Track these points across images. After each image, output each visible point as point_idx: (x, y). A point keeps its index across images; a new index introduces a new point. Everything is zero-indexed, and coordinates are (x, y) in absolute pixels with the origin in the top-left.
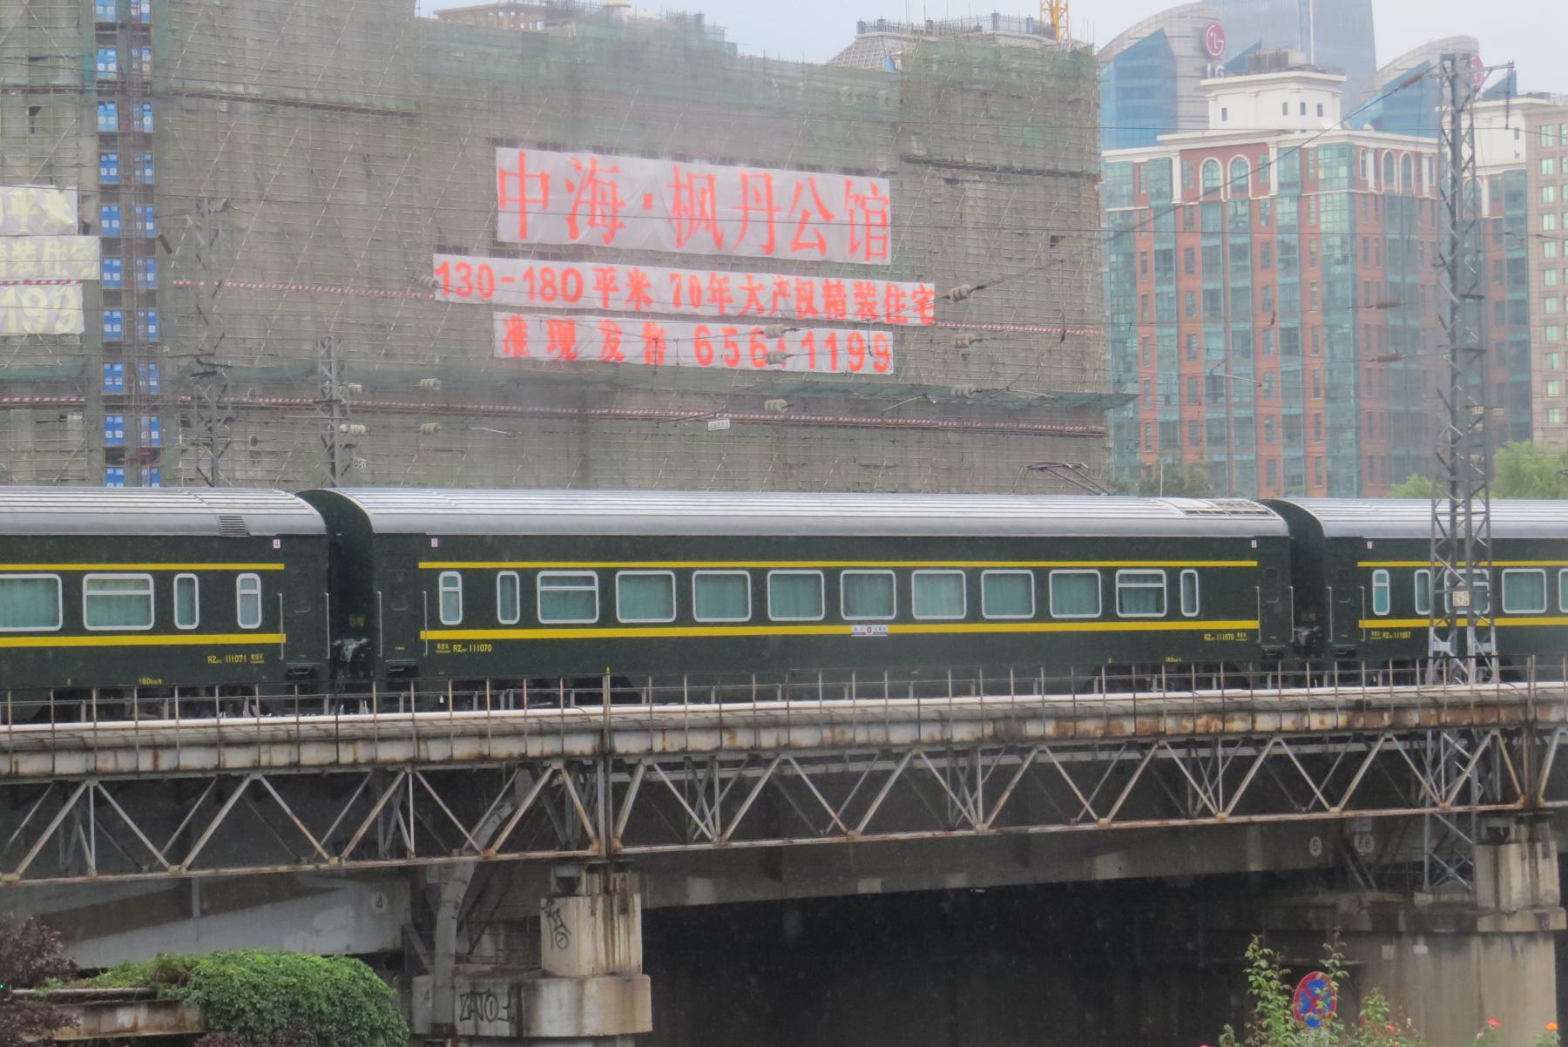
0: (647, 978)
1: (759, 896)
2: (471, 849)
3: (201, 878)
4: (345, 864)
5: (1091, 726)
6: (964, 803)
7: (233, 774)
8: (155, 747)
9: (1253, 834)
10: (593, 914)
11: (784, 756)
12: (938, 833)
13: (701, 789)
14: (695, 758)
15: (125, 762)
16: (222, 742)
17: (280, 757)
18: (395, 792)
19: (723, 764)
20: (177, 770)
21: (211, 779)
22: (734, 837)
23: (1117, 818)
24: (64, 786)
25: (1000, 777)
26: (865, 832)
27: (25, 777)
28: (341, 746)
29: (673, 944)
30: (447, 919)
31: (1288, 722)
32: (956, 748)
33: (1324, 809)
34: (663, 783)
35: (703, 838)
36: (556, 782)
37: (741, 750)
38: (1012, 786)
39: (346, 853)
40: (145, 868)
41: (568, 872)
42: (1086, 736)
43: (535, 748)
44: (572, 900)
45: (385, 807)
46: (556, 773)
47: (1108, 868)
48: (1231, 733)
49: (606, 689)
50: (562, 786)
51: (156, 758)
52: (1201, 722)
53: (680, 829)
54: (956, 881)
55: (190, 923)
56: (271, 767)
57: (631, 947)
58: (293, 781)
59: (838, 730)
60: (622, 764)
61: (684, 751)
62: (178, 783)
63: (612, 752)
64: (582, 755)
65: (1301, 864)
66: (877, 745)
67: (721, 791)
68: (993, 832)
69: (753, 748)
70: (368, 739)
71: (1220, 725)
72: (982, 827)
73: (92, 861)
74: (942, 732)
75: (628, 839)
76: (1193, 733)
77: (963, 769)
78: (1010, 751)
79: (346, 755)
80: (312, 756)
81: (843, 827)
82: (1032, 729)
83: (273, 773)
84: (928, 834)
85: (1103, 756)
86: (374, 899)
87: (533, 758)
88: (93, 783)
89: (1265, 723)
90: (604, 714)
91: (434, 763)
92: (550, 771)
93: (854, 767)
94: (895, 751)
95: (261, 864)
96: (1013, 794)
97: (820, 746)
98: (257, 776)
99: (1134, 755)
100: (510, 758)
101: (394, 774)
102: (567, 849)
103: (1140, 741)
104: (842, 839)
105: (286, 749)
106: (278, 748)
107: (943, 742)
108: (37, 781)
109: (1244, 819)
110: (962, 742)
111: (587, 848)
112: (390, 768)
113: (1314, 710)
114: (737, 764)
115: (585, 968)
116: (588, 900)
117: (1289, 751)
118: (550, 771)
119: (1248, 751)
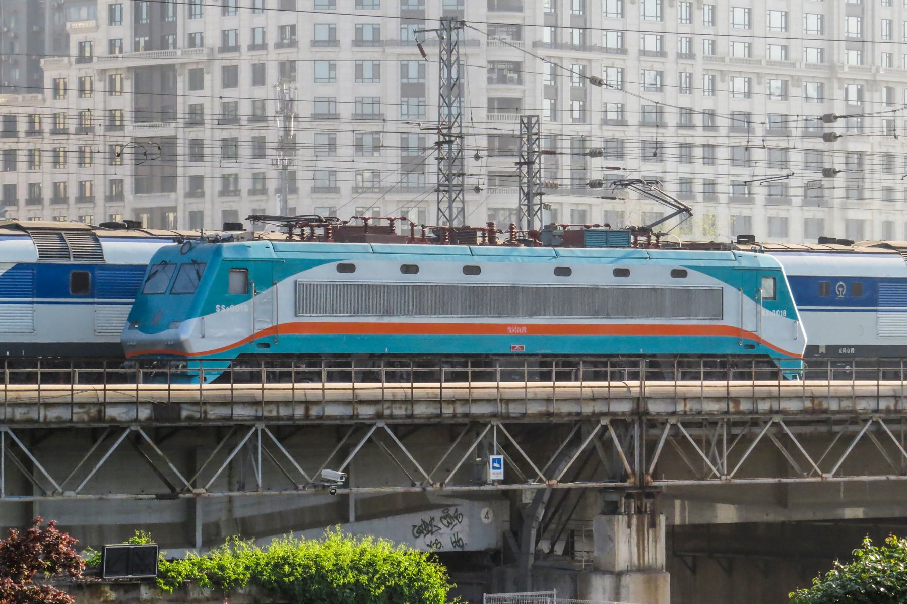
0: (668, 575)
3: (356, 494)
4: (449, 488)
8: (308, 404)
10: (629, 526)
11: (777, 418)
12: (893, 477)
13: (714, 441)
15: (284, 412)
16: (355, 401)
17: (399, 411)
18: (485, 436)
20: (321, 417)
21: (350, 426)
22: (735, 477)
24: (241, 428)
26: (837, 474)
27: (210, 420)
29: (692, 550)
34: (684, 437)
35: (715, 477)
36: (607, 434)
39: (447, 481)
40: (301, 486)
41: (614, 497)
43: (587, 409)
46: (605, 428)
49: (643, 369)
51: (307, 409)
55: (348, 525)
56: (391, 416)
57: (657, 552)
60: (654, 423)
61: (699, 413)
62: (338, 427)
63: (647, 413)
64: (624, 414)
66: (847, 412)
67: (730, 442)
69: (751, 413)
70: (465, 401)
74: (896, 405)
75: (655, 476)
79: (448, 410)
81: (820, 473)
84: (883, 478)
86: (484, 511)
87: (587, 416)
90: (641, 387)
91: (514, 418)
92: (599, 426)
94: (863, 417)
95: (395, 485)
98: (381, 424)
100: (570, 414)
101: (485, 425)
102: (613, 478)
104: (819, 479)
105: (404, 406)
106: (397, 405)
107: (897, 411)
108: (219, 424)
111: (625, 481)
112: (481, 421)
114: (742, 424)
116: (626, 517)
118: (599, 426)
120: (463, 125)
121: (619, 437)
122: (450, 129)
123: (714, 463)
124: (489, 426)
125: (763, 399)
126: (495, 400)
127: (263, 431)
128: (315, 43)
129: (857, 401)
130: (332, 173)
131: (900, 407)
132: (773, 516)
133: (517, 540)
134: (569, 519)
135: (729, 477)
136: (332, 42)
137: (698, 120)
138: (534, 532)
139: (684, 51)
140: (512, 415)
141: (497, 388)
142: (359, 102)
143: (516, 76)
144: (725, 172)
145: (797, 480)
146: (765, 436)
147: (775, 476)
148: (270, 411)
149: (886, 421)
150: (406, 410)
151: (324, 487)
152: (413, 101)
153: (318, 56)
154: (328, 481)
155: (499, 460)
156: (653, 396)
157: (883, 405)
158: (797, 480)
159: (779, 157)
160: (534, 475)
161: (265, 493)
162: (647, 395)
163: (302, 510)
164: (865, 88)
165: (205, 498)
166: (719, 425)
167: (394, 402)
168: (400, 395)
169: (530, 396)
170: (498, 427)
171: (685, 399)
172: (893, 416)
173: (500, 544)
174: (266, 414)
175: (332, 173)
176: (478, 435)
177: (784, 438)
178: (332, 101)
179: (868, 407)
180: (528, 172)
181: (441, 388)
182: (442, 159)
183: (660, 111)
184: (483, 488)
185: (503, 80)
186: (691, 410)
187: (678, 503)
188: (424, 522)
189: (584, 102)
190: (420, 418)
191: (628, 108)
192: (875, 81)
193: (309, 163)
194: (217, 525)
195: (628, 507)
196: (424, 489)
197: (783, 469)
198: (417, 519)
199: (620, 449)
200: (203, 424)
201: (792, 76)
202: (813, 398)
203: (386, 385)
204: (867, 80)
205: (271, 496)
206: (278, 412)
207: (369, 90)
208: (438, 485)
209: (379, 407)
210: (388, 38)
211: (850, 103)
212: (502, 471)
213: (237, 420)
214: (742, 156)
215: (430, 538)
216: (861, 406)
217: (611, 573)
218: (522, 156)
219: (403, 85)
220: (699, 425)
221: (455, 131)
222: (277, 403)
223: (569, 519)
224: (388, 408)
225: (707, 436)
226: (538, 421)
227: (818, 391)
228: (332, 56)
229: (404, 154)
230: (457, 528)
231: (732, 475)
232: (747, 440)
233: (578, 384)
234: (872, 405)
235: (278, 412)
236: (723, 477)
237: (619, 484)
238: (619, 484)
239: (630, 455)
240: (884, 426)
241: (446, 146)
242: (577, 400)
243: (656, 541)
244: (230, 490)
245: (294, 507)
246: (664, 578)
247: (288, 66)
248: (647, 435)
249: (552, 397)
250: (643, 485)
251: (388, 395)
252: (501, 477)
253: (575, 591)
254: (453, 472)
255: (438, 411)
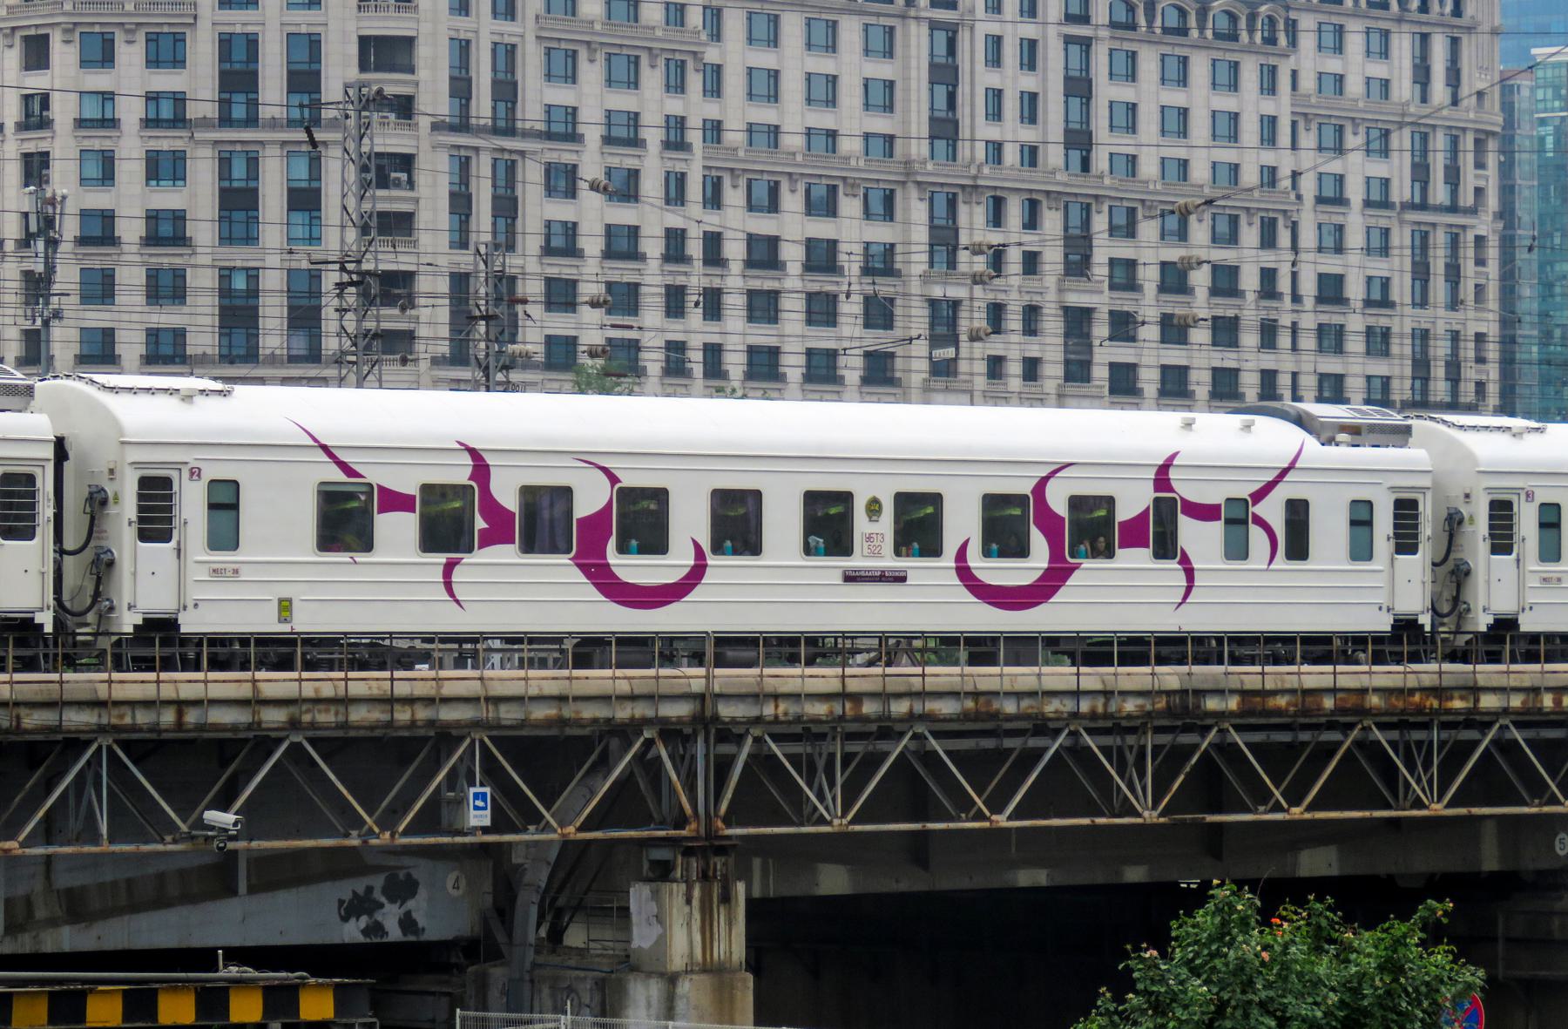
0: (750, 977)
1: (904, 886)
2: (547, 828)
5: (1282, 701)
6: (1133, 790)
7: (273, 734)
8: (181, 705)
9: (1489, 831)
10: (689, 901)
11: (920, 728)
13: (821, 764)
14: (815, 729)
15: (143, 718)
16: (256, 702)
17: (326, 717)
18: (461, 759)
19: (850, 737)
20: (201, 727)
21: (246, 740)
22: (856, 820)
23: (1309, 809)
24: (74, 744)
25: (1172, 759)
26: (1009, 818)
27: (27, 732)
28: (397, 707)
29: (786, 940)
30: (528, 907)
31: (1516, 702)
32: (1124, 723)
33: (1558, 803)
35: (822, 821)
36: (649, 756)
37: (866, 719)
38: (1188, 769)
40: (168, 838)
42: (1278, 712)
43: (623, 713)
44: (665, 887)
45: (448, 774)
46: (649, 743)
47: (1317, 862)
48: (1449, 712)
50: (659, 757)
51: (180, 714)
52: (1417, 698)
53: (800, 810)
54: (1135, 874)
56: (313, 725)
57: (733, 943)
58: (343, 746)
59: (982, 699)
60: (728, 733)
61: (798, 719)
62: (221, 743)
63: (716, 718)
64: (680, 720)
65: (1544, 865)
67: (845, 765)
68: (1162, 820)
69: (880, 718)
70: (429, 701)
71: (1436, 704)
72: (1150, 816)
73: (104, 829)
74: (1106, 705)
75: (728, 822)
76: (1403, 712)
77: (1131, 747)
78: (1187, 729)
79: (403, 715)
80: (358, 715)
81: (988, 813)
82: (1212, 704)
83: (320, 733)
84: (1086, 821)
85: (1305, 736)
88: (105, 741)
89: (1488, 702)
90: (707, 677)
93: (1008, 743)
94: (1051, 725)
96: (1187, 775)
97: (965, 716)
98: (297, 738)
99: (1334, 736)
100: (595, 721)
101: (461, 739)
102: (662, 824)
103: (1342, 719)
104: (986, 824)
105: (333, 709)
106: (322, 707)
107: (1107, 716)
109: (1463, 811)
110: (1129, 717)
112: (454, 732)
113: (1548, 689)
115: (677, 961)
116: (683, 887)
117: (1517, 735)
119: (1471, 735)
120: (380, 256)
121: (671, 757)
122: (359, 262)
123: (821, 797)
124: (468, 741)
125: (899, 696)
126: (477, 699)
127: (109, 748)
128: (81, 123)
129: (1046, 699)
130: (108, 335)
131: (1113, 708)
132: (908, 882)
133: (503, 922)
134: (588, 889)
135: (844, 821)
136: (111, 123)
137: (695, 248)
138: (534, 910)
139: (672, 138)
140: (504, 723)
141: (481, 679)
142: (153, 217)
143: (404, 176)
144: (737, 333)
145: (952, 825)
146: (902, 753)
147: (917, 821)
148: (122, 717)
149: (1090, 731)
150: (337, 714)
151: (207, 838)
152: (239, 216)
153: (87, 144)
154: (212, 828)
155: (484, 795)
156: (725, 691)
157: (1085, 706)
158: (952, 825)
159: (822, 310)
160: (535, 818)
161: (116, 848)
162: (717, 689)
163: (161, 877)
164: (960, 198)
165: (16, 857)
166: (829, 737)
167: (317, 701)
168: (327, 691)
169: (533, 691)
170: (482, 742)
171: (776, 697)
172: (1101, 724)
173: (476, 929)
174: (114, 721)
175: (108, 335)
176: (449, 756)
177: (930, 758)
178: (108, 217)
179: (1062, 708)
180: (487, 333)
181: (392, 679)
182: (346, 310)
183: (634, 232)
184: (459, 839)
185: (383, 182)
186: (786, 714)
187: (757, 863)
188: (354, 892)
189: (514, 218)
190: (358, 728)
191: (583, 229)
192: (976, 187)
193: (135, 317)
194: (28, 902)
195: (687, 869)
196: (365, 842)
197: (922, 808)
198: (346, 889)
199: (674, 777)
200: (13, 738)
201: (844, 179)
202: (976, 695)
203: (305, 675)
204: (963, 187)
205: (122, 854)
206: (134, 717)
207: (167, 198)
208: (387, 835)
209: (293, 709)
210: (200, 115)
211: (936, 222)
212: (488, 812)
213: (69, 732)
214: (764, 307)
215: (364, 921)
216: (1052, 707)
217: (662, 975)
218: (478, 306)
219: (222, 191)
220: (795, 738)
221: (365, 266)
222: (132, 704)
223: (588, 889)
224: (308, 711)
225: (810, 756)
226: (543, 733)
227: (984, 685)
228: (107, 145)
229: (226, 302)
230: (410, 904)
231: (849, 817)
232: (874, 761)
233: (608, 672)
234: (1068, 706)
235: (134, 717)
236: (836, 822)
237: (672, 833)
238: (672, 833)
239: (691, 789)
240: (1089, 740)
241: (353, 290)
242: (605, 699)
243: (730, 924)
244: (49, 843)
245: (151, 871)
246: (744, 981)
247: (36, 158)
248: (716, 756)
249: (565, 692)
250: (711, 834)
251: (308, 690)
252: (487, 822)
253: (603, 1004)
254: (411, 815)
255: (385, 717)
